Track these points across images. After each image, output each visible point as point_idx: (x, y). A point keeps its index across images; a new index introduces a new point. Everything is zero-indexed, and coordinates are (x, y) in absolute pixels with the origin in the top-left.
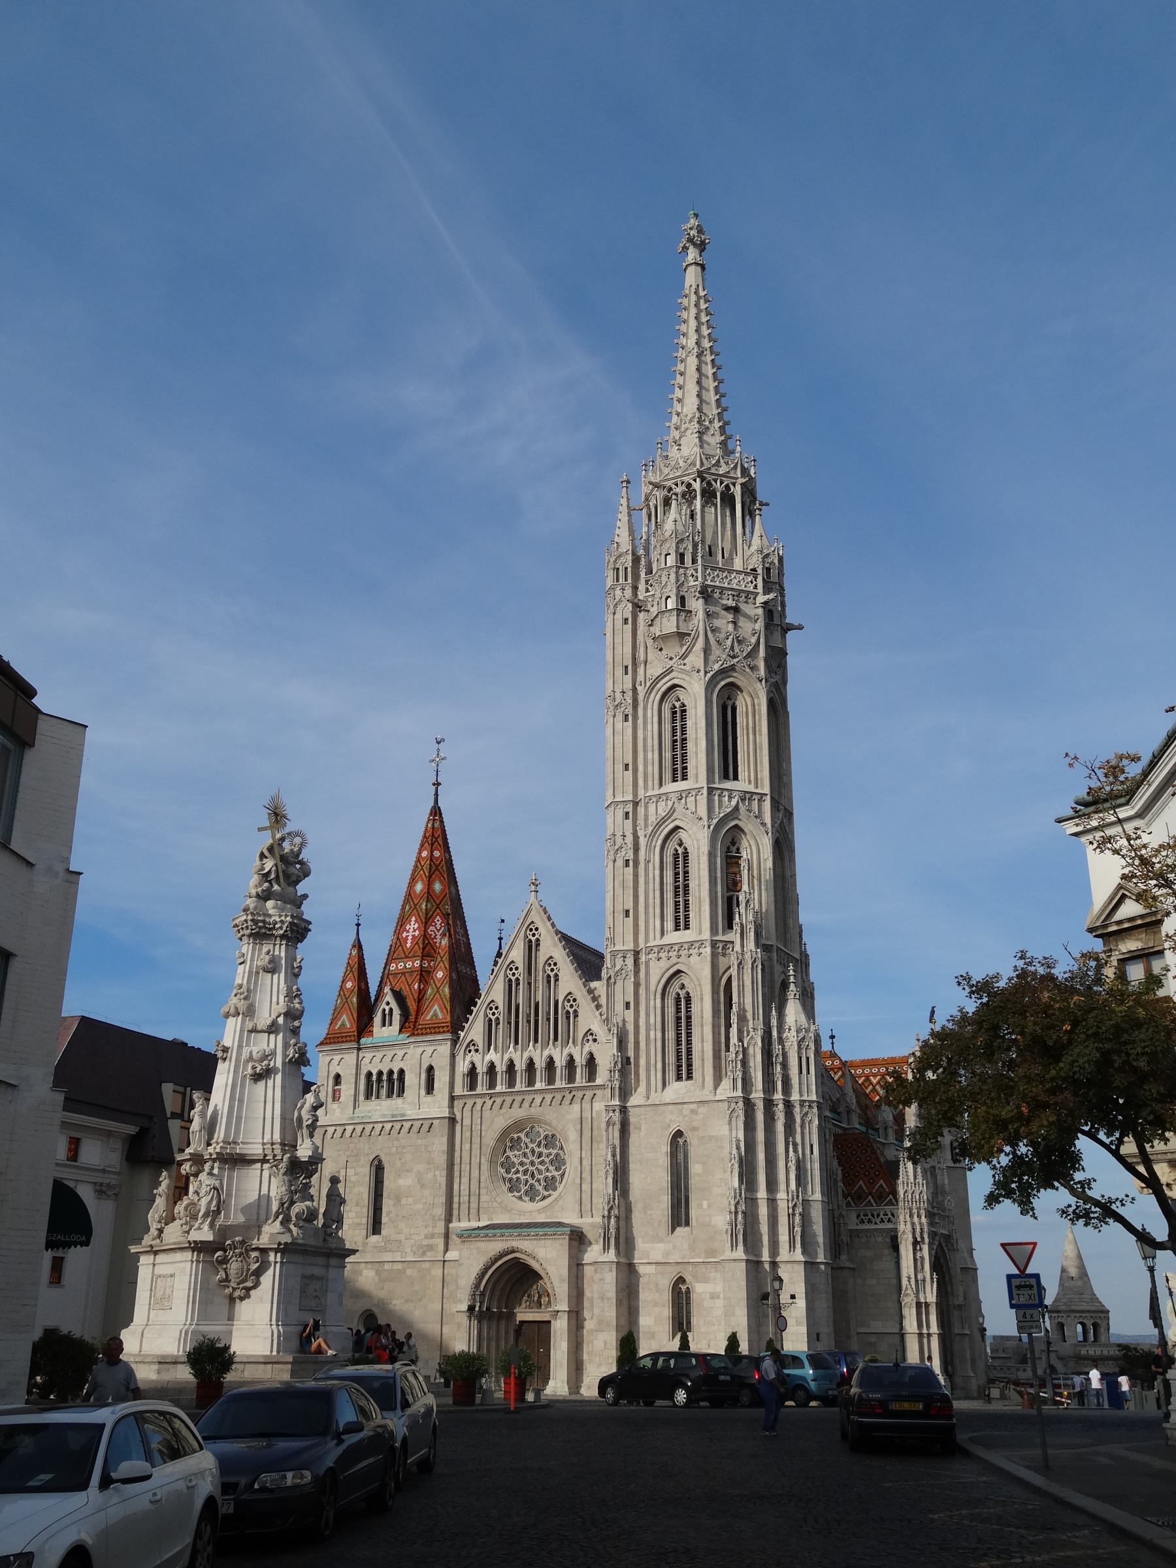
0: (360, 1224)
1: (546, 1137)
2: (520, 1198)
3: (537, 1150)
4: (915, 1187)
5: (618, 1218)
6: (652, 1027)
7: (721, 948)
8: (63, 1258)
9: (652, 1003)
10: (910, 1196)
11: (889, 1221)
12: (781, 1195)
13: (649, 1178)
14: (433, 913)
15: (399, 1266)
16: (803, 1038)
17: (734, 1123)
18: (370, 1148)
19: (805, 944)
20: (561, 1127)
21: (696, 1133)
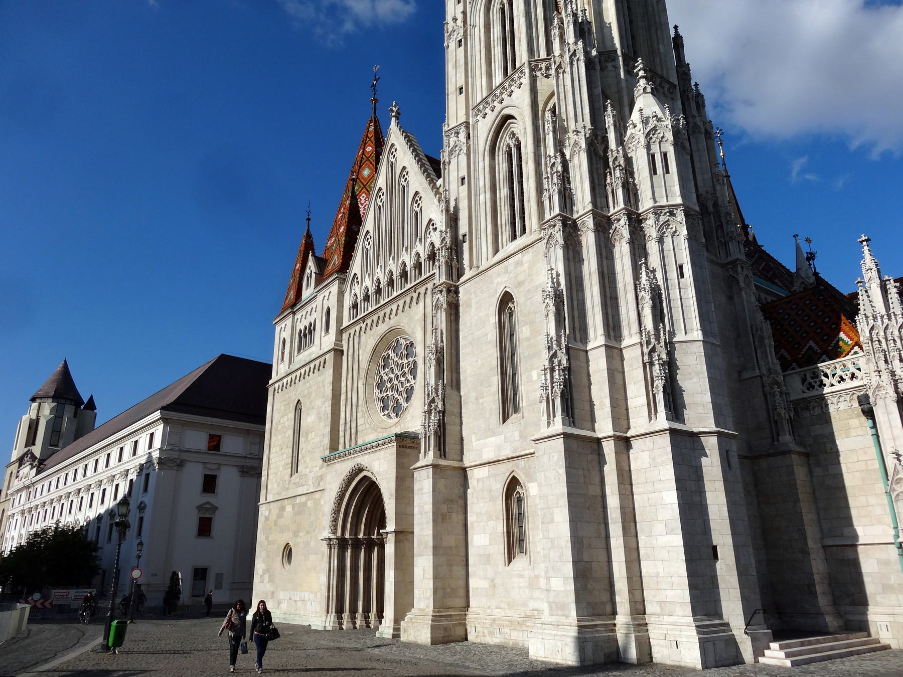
0: (287, 464)
1: (407, 347)
2: (389, 416)
3: (400, 362)
4: (890, 319)
5: (444, 412)
6: (482, 190)
7: (544, 69)
8: (211, 518)
9: (481, 164)
10: (882, 333)
11: (853, 376)
12: (630, 338)
13: (479, 360)
14: (360, 192)
15: (304, 498)
16: (655, 129)
17: (552, 254)
18: (295, 394)
19: (696, 85)
20: (411, 331)
21: (522, 289)
